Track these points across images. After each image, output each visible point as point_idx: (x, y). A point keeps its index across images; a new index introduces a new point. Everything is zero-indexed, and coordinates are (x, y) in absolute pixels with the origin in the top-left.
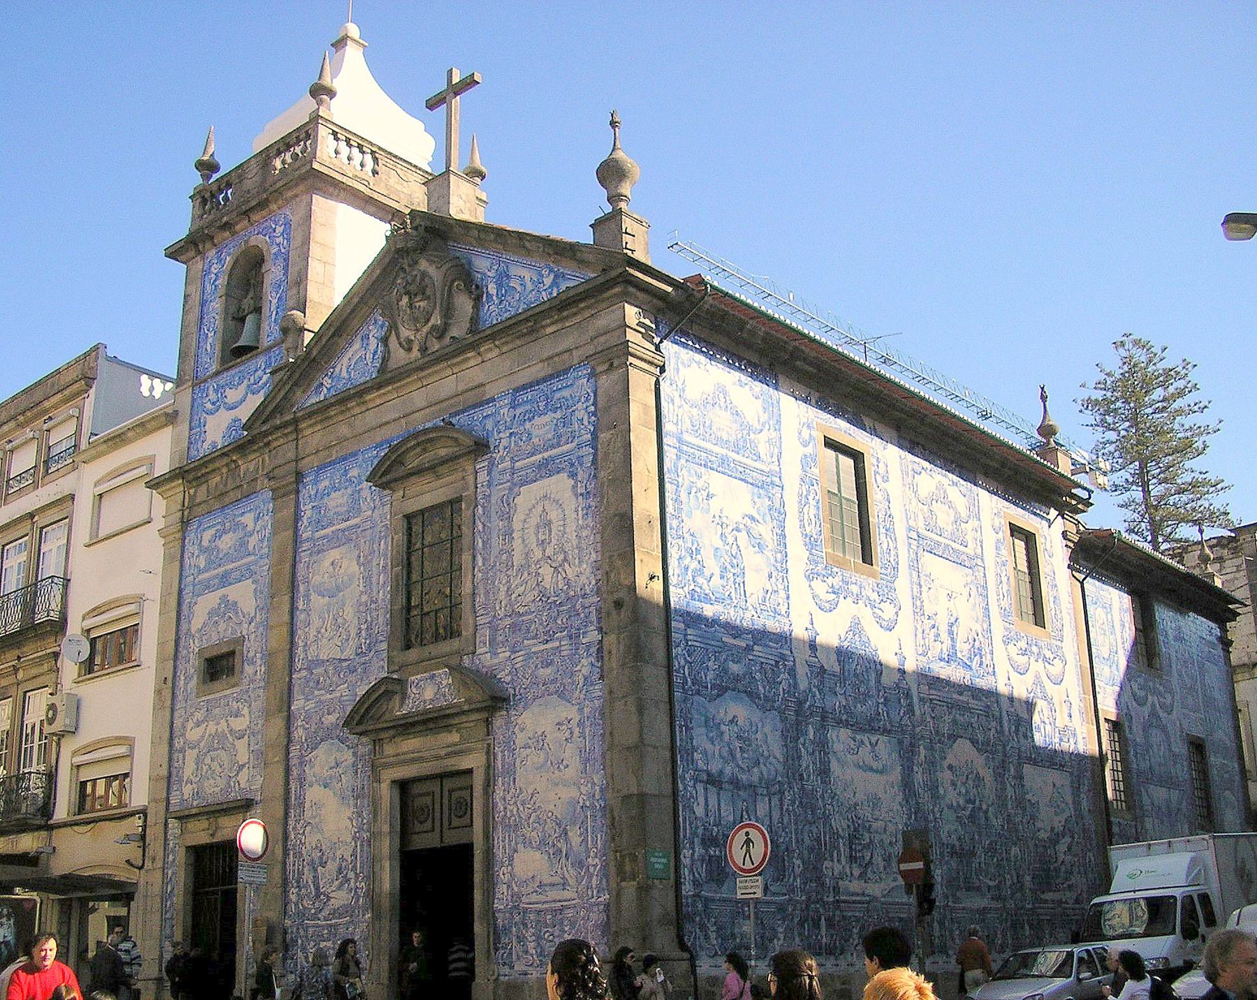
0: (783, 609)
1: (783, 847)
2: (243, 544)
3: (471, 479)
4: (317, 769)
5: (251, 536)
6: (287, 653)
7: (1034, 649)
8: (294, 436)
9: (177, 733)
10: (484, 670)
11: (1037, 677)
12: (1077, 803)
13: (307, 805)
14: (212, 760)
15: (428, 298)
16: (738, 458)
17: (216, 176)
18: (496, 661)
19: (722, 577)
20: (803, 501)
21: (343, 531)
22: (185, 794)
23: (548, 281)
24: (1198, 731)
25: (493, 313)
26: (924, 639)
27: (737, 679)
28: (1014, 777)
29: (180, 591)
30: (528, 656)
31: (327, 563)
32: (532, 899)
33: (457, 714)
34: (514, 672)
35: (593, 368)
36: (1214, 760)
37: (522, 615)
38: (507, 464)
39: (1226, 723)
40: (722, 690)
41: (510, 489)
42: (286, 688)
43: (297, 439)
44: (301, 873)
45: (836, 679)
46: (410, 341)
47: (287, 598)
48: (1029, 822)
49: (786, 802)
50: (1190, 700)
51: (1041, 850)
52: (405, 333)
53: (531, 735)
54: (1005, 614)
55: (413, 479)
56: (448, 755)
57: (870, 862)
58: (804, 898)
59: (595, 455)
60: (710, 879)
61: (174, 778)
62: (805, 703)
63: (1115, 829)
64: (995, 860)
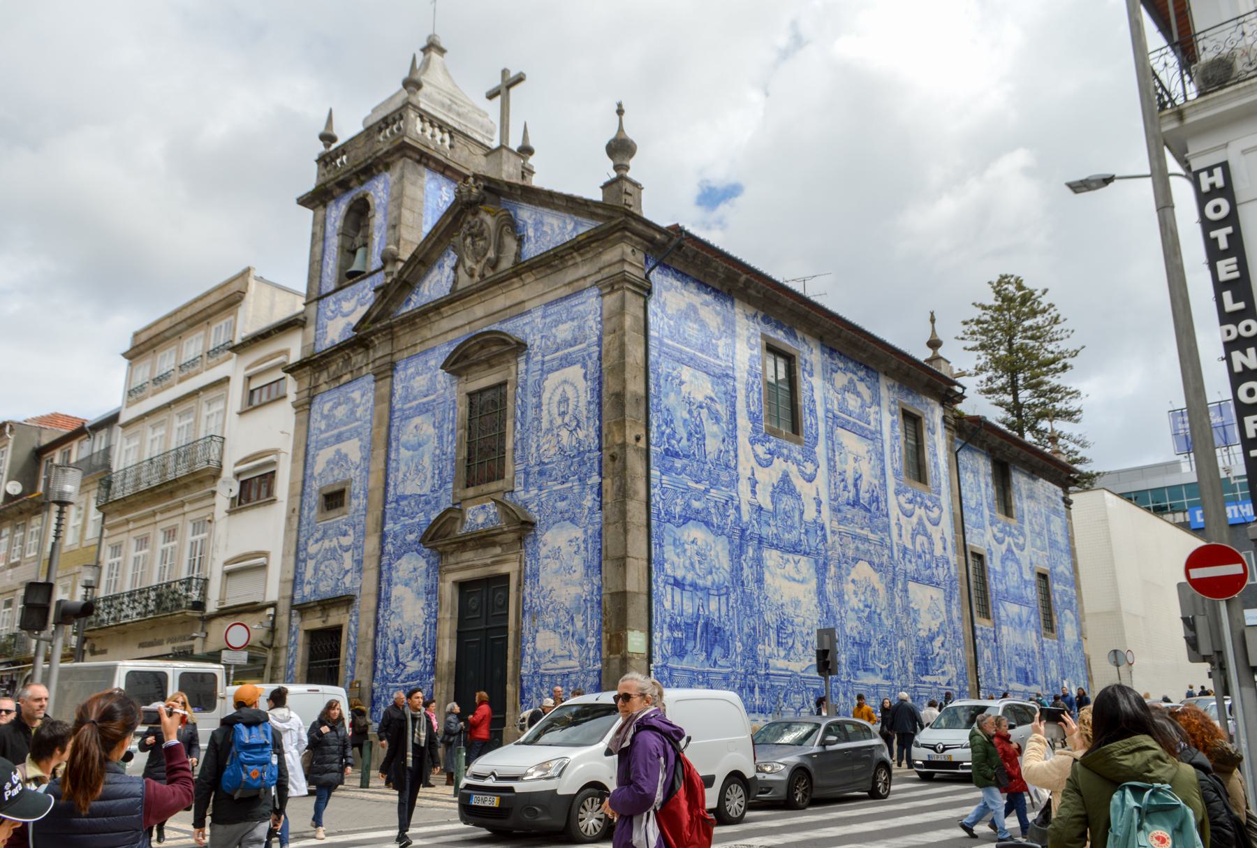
0: (733, 465)
1: (728, 633)
2: (353, 412)
3: (513, 368)
4: (400, 574)
5: (358, 407)
6: (381, 490)
7: (919, 499)
8: (390, 337)
9: (301, 547)
10: (520, 503)
11: (920, 519)
12: (949, 611)
13: (393, 599)
14: (326, 567)
15: (485, 239)
16: (704, 356)
17: (334, 146)
18: (528, 496)
19: (688, 440)
20: (750, 387)
21: (424, 404)
22: (306, 592)
23: (570, 227)
24: (1044, 566)
25: (532, 250)
27: (698, 512)
29: (307, 446)
30: (550, 493)
31: (412, 427)
32: (547, 666)
33: (499, 534)
34: (540, 505)
35: (600, 289)
36: (1057, 587)
37: (547, 464)
38: (539, 358)
39: (1066, 560)
40: (686, 520)
41: (541, 375)
42: (380, 515)
43: (392, 339)
44: (386, 649)
46: (472, 269)
47: (382, 452)
49: (731, 601)
50: (1038, 543)
51: (921, 644)
52: (469, 263)
53: (550, 548)
54: (896, 474)
55: (475, 368)
56: (494, 563)
57: (792, 647)
58: (743, 671)
59: (600, 352)
60: (675, 654)
61: (298, 581)
63: (978, 633)
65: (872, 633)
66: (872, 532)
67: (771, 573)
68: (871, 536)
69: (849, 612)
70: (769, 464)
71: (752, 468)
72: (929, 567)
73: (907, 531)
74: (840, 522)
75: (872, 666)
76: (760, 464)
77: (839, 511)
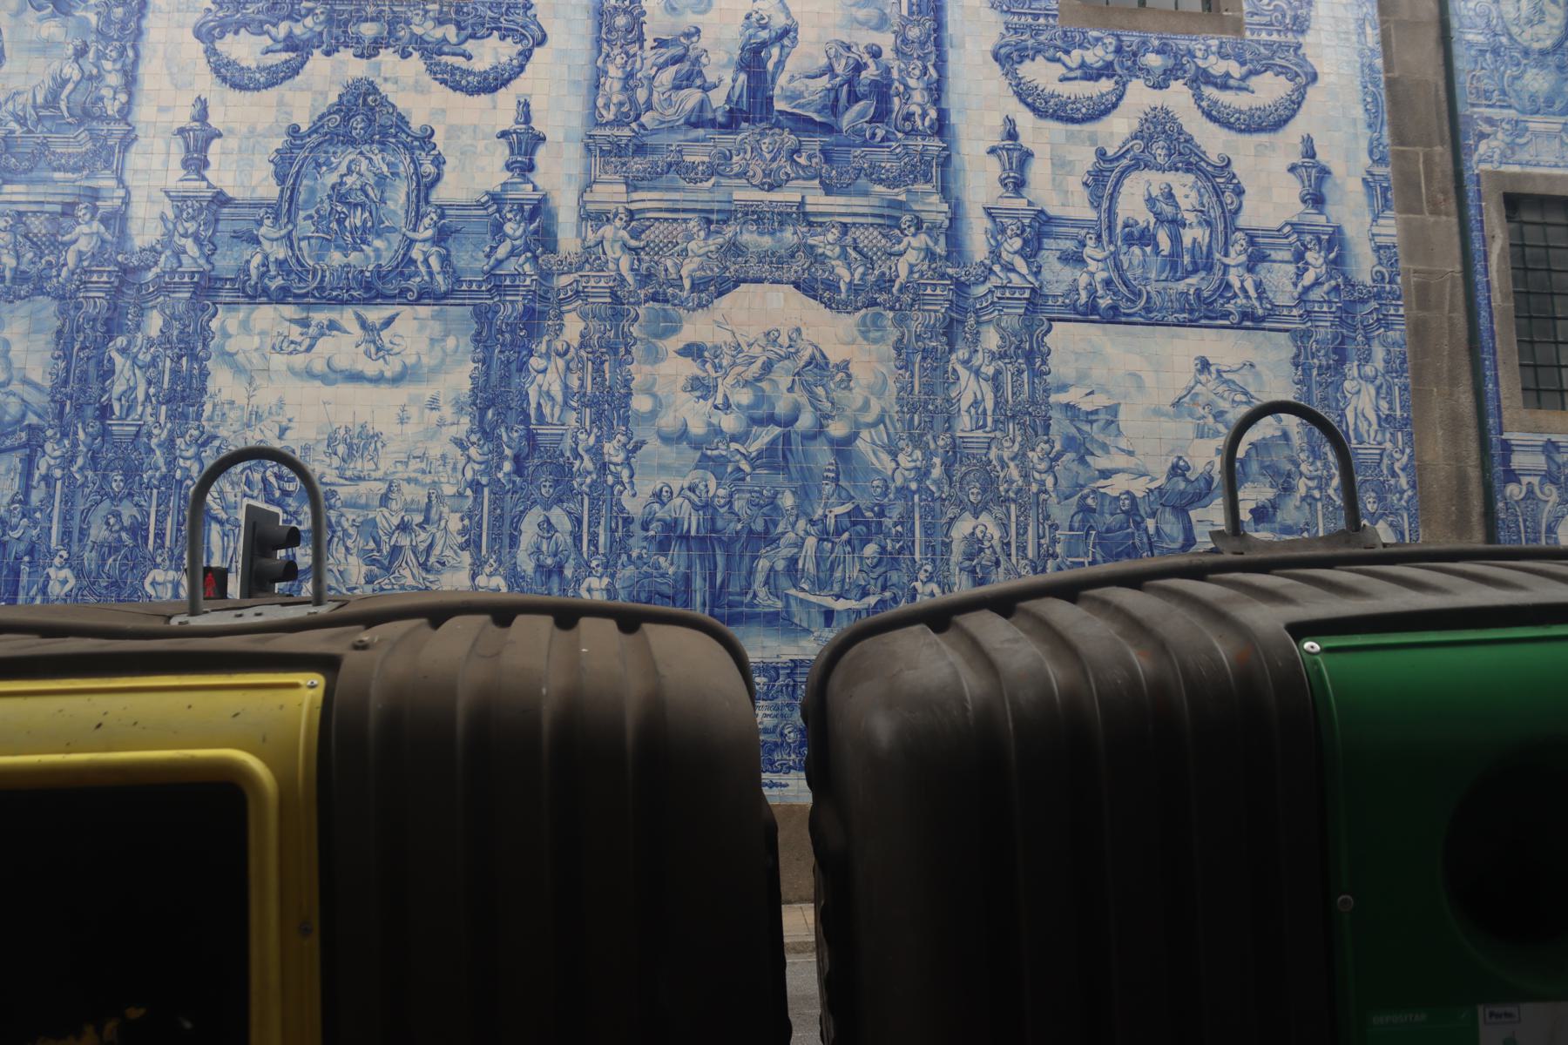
0: (112, 108)
1: (22, 547)
7: (1153, 60)
26: (625, 88)
28: (994, 356)
45: (262, 212)
62: (149, 268)
64: (871, 550)
65: (788, 501)
66: (828, 190)
67: (238, 370)
68: (818, 201)
69: (653, 445)
70: (276, 77)
72: (1205, 263)
73: (1060, 165)
74: (632, 186)
75: (766, 601)
76: (234, 86)
77: (640, 150)
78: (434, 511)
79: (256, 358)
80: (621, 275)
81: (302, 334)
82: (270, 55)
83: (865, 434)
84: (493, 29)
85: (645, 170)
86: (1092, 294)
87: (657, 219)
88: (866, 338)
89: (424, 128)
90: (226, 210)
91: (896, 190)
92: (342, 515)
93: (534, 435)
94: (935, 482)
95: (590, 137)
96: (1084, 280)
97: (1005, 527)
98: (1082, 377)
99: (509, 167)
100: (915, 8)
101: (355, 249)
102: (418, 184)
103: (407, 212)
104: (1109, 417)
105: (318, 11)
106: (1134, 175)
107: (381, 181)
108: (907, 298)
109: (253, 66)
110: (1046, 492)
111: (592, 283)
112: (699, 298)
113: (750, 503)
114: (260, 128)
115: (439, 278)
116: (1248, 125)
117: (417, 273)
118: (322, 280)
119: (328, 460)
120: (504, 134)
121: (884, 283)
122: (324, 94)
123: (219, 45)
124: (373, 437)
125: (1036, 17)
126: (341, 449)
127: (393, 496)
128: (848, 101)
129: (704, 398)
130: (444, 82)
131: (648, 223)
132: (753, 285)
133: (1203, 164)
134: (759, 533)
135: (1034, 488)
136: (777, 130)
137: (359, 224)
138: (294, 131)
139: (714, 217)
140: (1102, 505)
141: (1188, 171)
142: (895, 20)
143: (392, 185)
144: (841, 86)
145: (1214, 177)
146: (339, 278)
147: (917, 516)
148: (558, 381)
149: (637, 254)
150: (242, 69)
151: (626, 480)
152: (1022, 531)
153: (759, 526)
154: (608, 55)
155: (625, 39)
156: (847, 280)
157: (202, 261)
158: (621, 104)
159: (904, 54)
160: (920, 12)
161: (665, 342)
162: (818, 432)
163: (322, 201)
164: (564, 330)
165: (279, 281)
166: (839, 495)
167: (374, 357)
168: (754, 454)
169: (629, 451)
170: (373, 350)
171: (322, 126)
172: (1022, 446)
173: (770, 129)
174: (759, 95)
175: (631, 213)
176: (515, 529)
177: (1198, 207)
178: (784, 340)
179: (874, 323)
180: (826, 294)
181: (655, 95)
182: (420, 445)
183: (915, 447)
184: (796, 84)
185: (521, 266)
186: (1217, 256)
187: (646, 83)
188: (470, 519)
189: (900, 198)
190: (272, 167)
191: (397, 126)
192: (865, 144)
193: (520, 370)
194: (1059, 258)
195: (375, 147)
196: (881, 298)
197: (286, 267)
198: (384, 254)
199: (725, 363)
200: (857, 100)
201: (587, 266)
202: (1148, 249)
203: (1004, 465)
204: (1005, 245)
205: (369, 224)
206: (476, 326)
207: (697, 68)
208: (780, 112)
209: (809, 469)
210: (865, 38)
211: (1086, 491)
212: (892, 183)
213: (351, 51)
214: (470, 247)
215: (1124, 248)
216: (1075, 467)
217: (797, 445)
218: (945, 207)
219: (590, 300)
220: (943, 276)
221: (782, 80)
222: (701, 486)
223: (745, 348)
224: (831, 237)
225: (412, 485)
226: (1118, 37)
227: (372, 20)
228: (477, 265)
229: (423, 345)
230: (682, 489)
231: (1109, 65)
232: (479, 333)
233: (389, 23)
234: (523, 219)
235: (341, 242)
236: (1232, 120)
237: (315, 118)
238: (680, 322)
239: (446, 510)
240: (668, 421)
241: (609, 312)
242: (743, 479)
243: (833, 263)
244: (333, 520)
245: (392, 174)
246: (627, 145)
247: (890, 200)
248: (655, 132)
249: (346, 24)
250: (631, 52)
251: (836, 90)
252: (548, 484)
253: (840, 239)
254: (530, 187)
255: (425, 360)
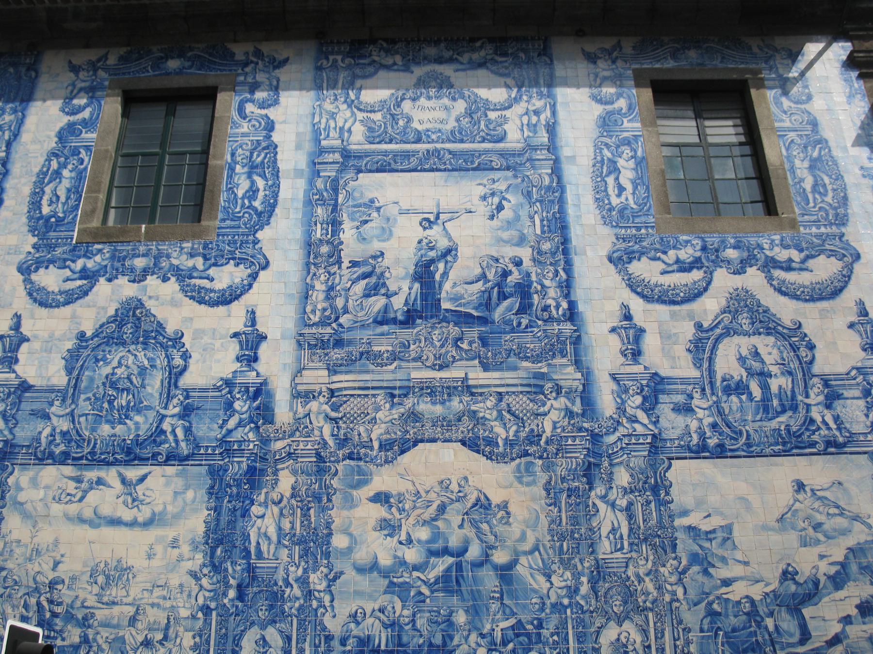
7: (731, 254)
26: (328, 298)
28: (625, 491)
45: (53, 396)
48: (684, 572)
65: (461, 618)
66: (486, 367)
67: (26, 516)
68: (478, 376)
69: (350, 574)
70: (70, 297)
71: (18, 317)
73: (666, 337)
74: (332, 370)
76: (43, 304)
77: (339, 343)
78: (171, 630)
79: (40, 507)
80: (323, 439)
81: (76, 488)
82: (69, 282)
83: (523, 560)
84: (230, 259)
85: (342, 359)
86: (702, 436)
87: (352, 395)
88: (521, 483)
89: (176, 332)
90: (27, 395)
91: (539, 365)
92: (98, 633)
93: (254, 568)
94: (583, 597)
95: (301, 335)
96: (694, 425)
97: (645, 632)
98: (700, 503)
99: (238, 359)
100: (546, 228)
101: (120, 423)
102: (170, 374)
103: (161, 394)
104: (725, 535)
105: (105, 251)
106: (726, 340)
107: (143, 371)
108: (552, 449)
109: (56, 290)
110: (678, 600)
111: (301, 446)
112: (386, 456)
113: (430, 621)
114: (58, 334)
115: (183, 444)
116: (812, 296)
117: (166, 441)
118: (94, 447)
119: (89, 588)
120: (236, 335)
121: (534, 438)
122: (105, 309)
123: (34, 277)
124: (126, 570)
125: (639, 229)
126: (101, 579)
127: (139, 617)
128: (499, 300)
129: (391, 535)
130: (192, 298)
131: (345, 399)
132: (428, 444)
133: (779, 328)
134: (438, 646)
135: (667, 598)
136: (444, 324)
137: (124, 404)
138: (81, 336)
139: (397, 392)
140: (726, 609)
141: (768, 334)
142: (532, 238)
143: (150, 375)
144: (493, 288)
145: (790, 337)
146: (107, 445)
147: (570, 627)
148: (274, 524)
149: (336, 423)
150: (49, 292)
151: (327, 604)
152: (660, 634)
153: (438, 640)
154: (315, 274)
155: (328, 262)
156: (504, 437)
157: (6, 433)
158: (324, 310)
159: (540, 262)
160: (550, 231)
161: (358, 491)
162: (485, 560)
163: (98, 387)
164: (279, 483)
165: (62, 448)
166: (504, 612)
167: (130, 506)
168: (432, 580)
169: (330, 580)
170: (130, 500)
171: (102, 332)
172: (654, 563)
173: (439, 323)
174: (430, 298)
175: (332, 392)
176: (237, 645)
177: (780, 361)
178: (454, 487)
179: (527, 470)
180: (487, 449)
181: (350, 301)
182: (163, 576)
183: (566, 569)
184: (458, 289)
185: (246, 434)
186: (800, 398)
187: (343, 293)
188: (201, 636)
189: (542, 370)
190: (63, 362)
191: (157, 331)
192: (513, 331)
193: (243, 516)
194: (673, 410)
195: (139, 346)
196: (532, 449)
197: (68, 437)
198: (142, 426)
199: (407, 507)
200: (505, 298)
201: (298, 433)
202: (744, 397)
203: (640, 580)
204: (629, 402)
205: (132, 404)
206: (210, 482)
207: (382, 281)
208: (447, 310)
209: (478, 591)
210: (509, 252)
211: (711, 598)
212: (537, 359)
213: (127, 278)
214: (207, 421)
215: (724, 398)
216: (700, 578)
217: (468, 571)
218: (579, 375)
219: (300, 460)
220: (580, 429)
221: (447, 286)
222: (389, 608)
223: (423, 494)
224: (489, 404)
225: (155, 609)
226: (703, 239)
227: (143, 255)
228: (213, 434)
229: (169, 498)
230: (374, 610)
231: (698, 260)
232: (212, 487)
233: (155, 258)
234: (249, 398)
235: (110, 417)
236: (798, 293)
237: (98, 326)
238: (371, 475)
239: (181, 629)
240: (362, 556)
241: (314, 469)
242: (424, 601)
243: (492, 424)
244: (91, 637)
245: (151, 366)
246: (329, 340)
247: (535, 373)
248: (350, 329)
249: (124, 259)
250: (332, 271)
251: (489, 291)
252: (264, 608)
253: (497, 405)
254: (254, 373)
255: (170, 508)
